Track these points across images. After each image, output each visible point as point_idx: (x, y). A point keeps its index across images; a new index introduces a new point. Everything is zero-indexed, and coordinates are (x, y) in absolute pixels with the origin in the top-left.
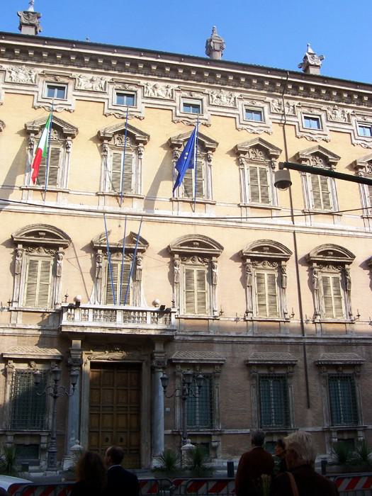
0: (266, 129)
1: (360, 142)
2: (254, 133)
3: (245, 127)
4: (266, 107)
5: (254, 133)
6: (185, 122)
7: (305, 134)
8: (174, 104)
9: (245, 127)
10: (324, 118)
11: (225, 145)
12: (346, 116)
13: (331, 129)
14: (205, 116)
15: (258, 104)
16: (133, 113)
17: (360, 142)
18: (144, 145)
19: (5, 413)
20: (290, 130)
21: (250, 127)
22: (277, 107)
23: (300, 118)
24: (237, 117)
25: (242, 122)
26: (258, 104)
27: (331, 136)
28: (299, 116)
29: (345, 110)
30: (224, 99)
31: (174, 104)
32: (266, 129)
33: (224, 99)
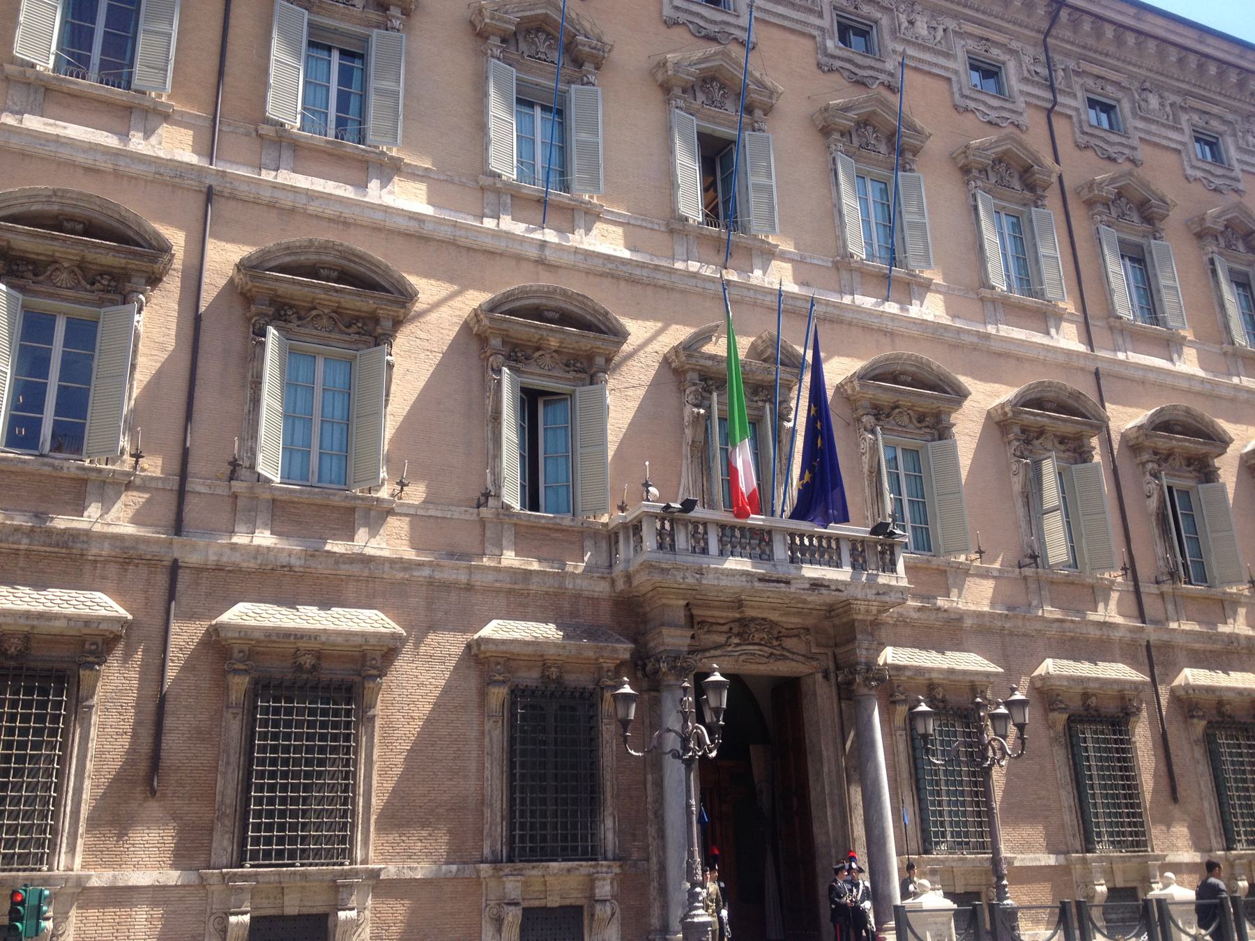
0: (1014, 117)
1: (1199, 174)
2: (990, 123)
3: (972, 105)
4: (1011, 65)
5: (990, 123)
6: (846, 74)
7: (1093, 141)
8: (818, 22)
9: (972, 105)
10: (1126, 106)
11: (937, 145)
12: (1168, 109)
13: (1143, 135)
14: (890, 65)
15: (995, 52)
16: (732, 30)
17: (1199, 174)
18: (765, 115)
19: (487, 813)
20: (1060, 126)
21: (982, 108)
22: (1032, 68)
23: (1079, 102)
24: (954, 78)
25: (967, 92)
26: (995, 52)
27: (1143, 153)
28: (1079, 94)
29: (1166, 94)
30: (922, 28)
31: (818, 22)
32: (1014, 117)
33: (922, 28)
